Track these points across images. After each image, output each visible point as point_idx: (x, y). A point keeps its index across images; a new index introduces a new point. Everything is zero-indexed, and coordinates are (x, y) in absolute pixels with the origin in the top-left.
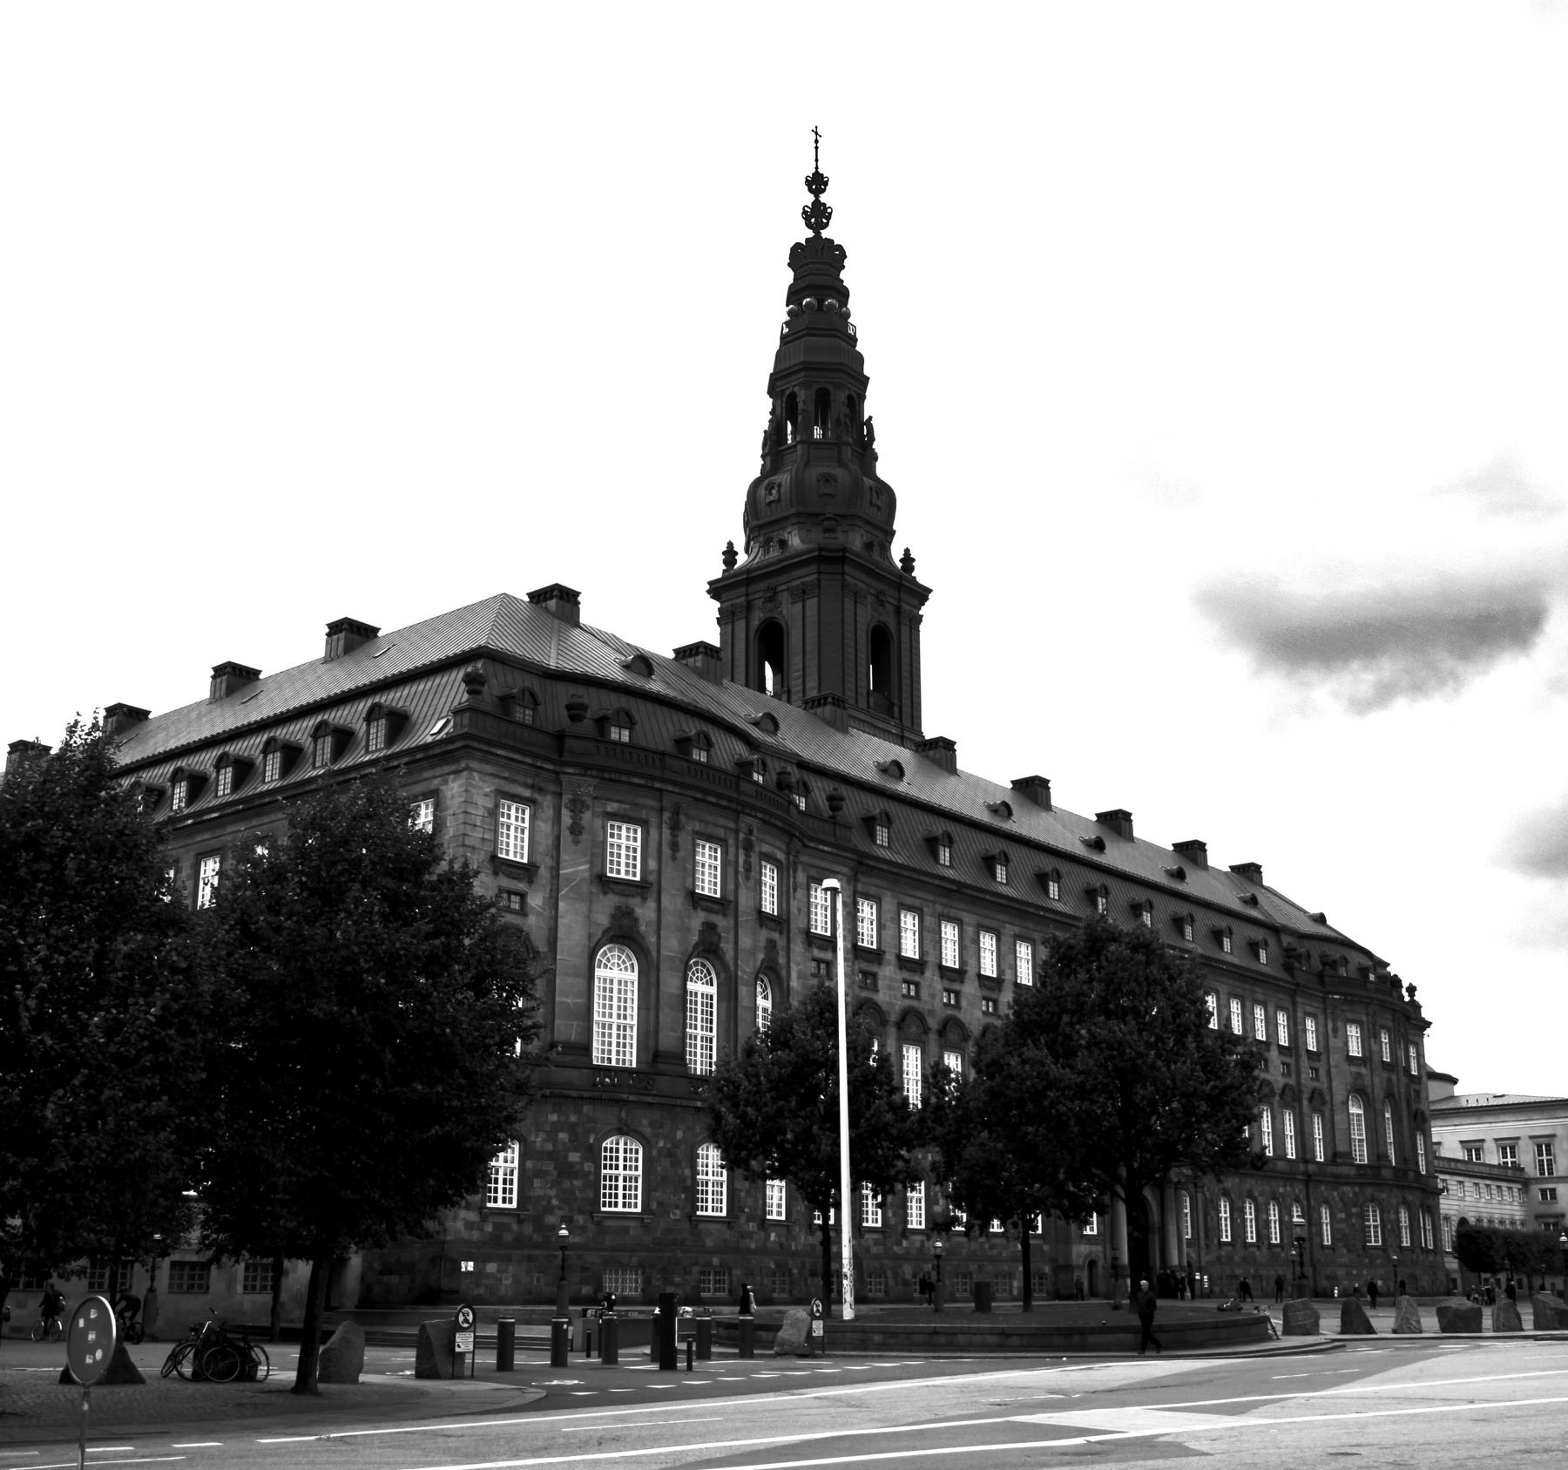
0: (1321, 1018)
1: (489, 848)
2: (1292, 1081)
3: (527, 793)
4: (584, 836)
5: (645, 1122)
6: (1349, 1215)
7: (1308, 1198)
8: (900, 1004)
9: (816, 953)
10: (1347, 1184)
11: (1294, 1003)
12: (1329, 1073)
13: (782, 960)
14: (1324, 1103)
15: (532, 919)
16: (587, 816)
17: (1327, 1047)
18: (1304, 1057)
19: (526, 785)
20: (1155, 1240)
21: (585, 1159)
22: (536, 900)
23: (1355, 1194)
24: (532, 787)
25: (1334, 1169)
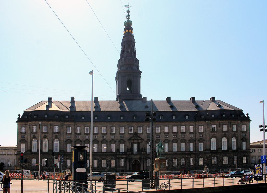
0: (205, 126)
1: (20, 132)
2: (194, 138)
3: (25, 125)
4: (30, 129)
5: (36, 157)
6: (208, 159)
7: (195, 157)
8: (84, 139)
9: (68, 135)
10: (207, 154)
11: (195, 124)
12: (206, 135)
13: (59, 137)
14: (204, 140)
15: (26, 138)
16: (30, 126)
17: (206, 131)
18: (198, 133)
19: (24, 125)
20: (140, 166)
21: (30, 161)
22: (26, 136)
23: (210, 156)
24: (25, 125)
25: (205, 152)
